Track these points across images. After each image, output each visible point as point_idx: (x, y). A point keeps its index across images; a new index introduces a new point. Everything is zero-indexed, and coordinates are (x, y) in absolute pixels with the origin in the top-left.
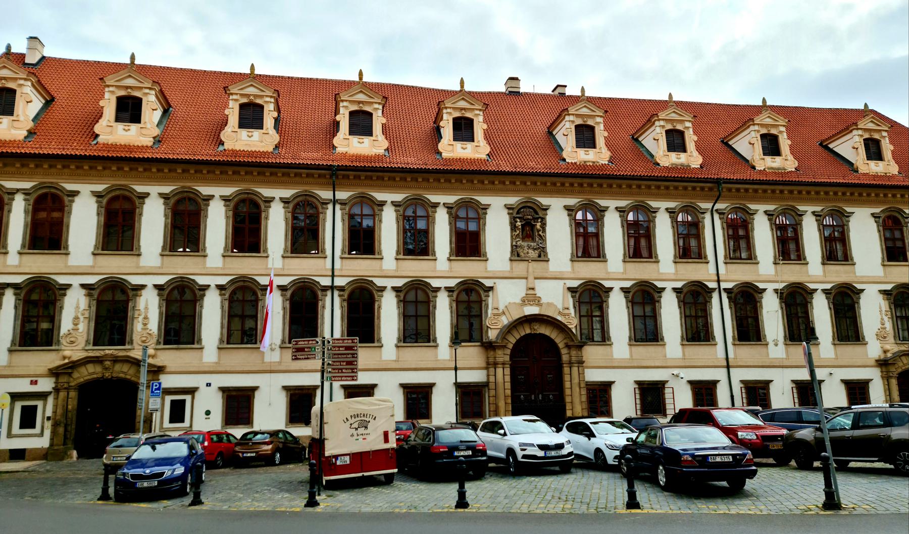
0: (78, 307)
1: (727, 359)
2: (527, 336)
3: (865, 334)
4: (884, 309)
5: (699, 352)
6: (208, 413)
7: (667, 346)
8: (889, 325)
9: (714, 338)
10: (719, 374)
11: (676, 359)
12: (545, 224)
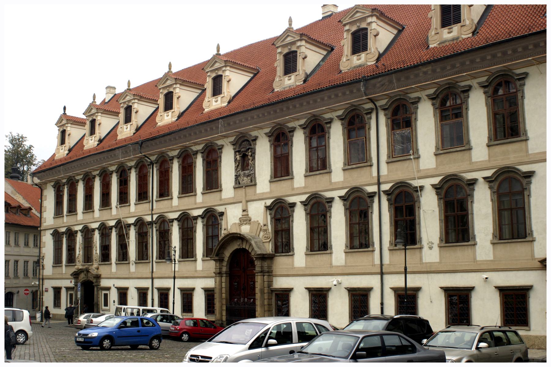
0: (80, 243)
1: (382, 265)
2: (237, 250)
6: (114, 302)
7: (334, 255)
9: (373, 245)
10: (373, 282)
11: (339, 266)
12: (254, 153)
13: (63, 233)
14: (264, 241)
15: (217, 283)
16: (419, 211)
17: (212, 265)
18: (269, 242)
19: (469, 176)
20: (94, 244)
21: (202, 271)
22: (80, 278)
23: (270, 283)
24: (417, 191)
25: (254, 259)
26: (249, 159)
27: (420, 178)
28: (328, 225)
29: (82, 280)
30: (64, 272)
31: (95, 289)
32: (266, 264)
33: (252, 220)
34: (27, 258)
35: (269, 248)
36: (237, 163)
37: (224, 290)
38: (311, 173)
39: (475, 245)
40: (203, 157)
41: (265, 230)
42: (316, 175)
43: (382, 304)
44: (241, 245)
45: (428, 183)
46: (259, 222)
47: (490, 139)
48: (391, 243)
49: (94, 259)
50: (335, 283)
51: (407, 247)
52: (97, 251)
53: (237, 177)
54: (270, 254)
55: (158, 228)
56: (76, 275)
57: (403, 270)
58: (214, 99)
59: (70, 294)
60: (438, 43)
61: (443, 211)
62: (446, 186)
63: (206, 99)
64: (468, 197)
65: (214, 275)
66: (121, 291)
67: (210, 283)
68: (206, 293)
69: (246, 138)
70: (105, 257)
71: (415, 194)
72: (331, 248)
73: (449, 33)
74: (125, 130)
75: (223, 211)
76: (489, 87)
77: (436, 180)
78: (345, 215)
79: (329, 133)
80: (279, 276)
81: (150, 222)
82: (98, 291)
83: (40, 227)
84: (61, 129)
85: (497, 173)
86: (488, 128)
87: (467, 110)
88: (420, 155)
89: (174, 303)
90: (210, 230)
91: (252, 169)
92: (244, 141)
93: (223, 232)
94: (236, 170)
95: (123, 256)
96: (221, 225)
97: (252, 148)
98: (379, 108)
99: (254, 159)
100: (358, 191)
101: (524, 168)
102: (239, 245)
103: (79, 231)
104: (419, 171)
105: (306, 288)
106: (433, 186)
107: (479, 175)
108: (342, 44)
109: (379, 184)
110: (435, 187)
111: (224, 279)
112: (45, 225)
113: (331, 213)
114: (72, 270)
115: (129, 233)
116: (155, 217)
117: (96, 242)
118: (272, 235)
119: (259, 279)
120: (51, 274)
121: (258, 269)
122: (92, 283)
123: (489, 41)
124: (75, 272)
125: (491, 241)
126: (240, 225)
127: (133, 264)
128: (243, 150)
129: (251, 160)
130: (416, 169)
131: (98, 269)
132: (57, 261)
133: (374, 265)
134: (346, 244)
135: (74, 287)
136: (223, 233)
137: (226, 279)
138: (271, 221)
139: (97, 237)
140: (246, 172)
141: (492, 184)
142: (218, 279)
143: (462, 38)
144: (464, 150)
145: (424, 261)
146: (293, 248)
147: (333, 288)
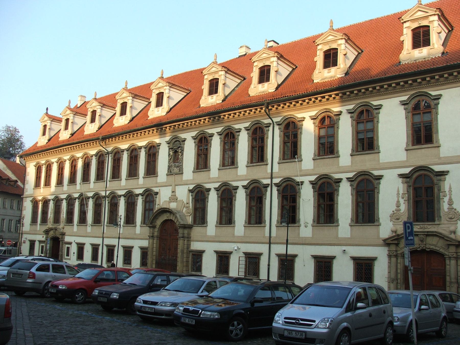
0: (51, 208)
2: (166, 221)
3: (380, 216)
4: (401, 192)
5: (255, 231)
6: (74, 253)
8: (403, 207)
10: (262, 248)
12: (183, 150)
13: (40, 201)
14: (186, 215)
15: (150, 244)
16: (299, 199)
17: (147, 230)
18: (190, 216)
19: (337, 176)
20: (62, 210)
21: (140, 234)
22: (50, 235)
23: (189, 246)
24: (299, 185)
25: (178, 228)
26: (179, 155)
27: (301, 176)
28: (233, 206)
29: (52, 236)
30: (38, 229)
31: (61, 243)
32: (186, 231)
33: (178, 199)
34: (11, 218)
35: (190, 220)
36: (170, 157)
37: (155, 249)
38: (223, 168)
39: (338, 226)
40: (145, 151)
41: (187, 207)
42: (227, 169)
43: (269, 265)
44: (169, 217)
45: (307, 179)
46: (183, 201)
47: (353, 150)
48: (278, 222)
49: (61, 221)
50: (236, 248)
51: (289, 225)
52: (64, 215)
53: (169, 167)
54: (190, 225)
55: (109, 201)
56: (47, 232)
57: (286, 242)
58: (156, 109)
59: (42, 246)
60: (320, 79)
61: (316, 201)
62: (320, 183)
63: (151, 109)
64: (335, 191)
65: (148, 238)
66: (79, 245)
67: (145, 243)
68: (142, 251)
69: (177, 139)
70: (70, 220)
71: (297, 187)
72: (234, 223)
73: (328, 73)
74: (90, 128)
75: (158, 191)
76: (354, 113)
77: (313, 178)
78: (246, 200)
79: (238, 139)
80: (196, 241)
81: (104, 196)
82: (62, 244)
83: (23, 195)
84: (44, 124)
85: (356, 175)
86: (352, 142)
87: (338, 128)
88: (302, 159)
89: (117, 257)
90: (147, 205)
91: (180, 162)
92: (176, 141)
93: (156, 207)
94: (169, 162)
95: (83, 220)
96: (156, 202)
97: (182, 147)
98: (275, 123)
99: (183, 154)
100: (256, 182)
101: (376, 173)
102: (168, 217)
103: (51, 200)
104: (301, 170)
105: (215, 251)
106: (311, 182)
107: (343, 176)
108: (251, 76)
109: (272, 178)
110: (312, 183)
111: (155, 241)
112: (26, 193)
113: (236, 197)
114: (45, 228)
115: (88, 203)
116: (108, 193)
117: (64, 208)
118: (192, 211)
119: (181, 242)
120: (29, 230)
121: (180, 235)
122: (58, 238)
123: (356, 81)
124: (47, 229)
125: (350, 224)
126: (170, 202)
127: (89, 226)
128: (175, 147)
129: (180, 155)
130: (299, 169)
131: (63, 228)
132: (34, 221)
133: (264, 237)
134: (245, 221)
135: (45, 241)
136: (157, 207)
137: (157, 242)
138: (192, 201)
139: (64, 205)
140: (176, 164)
141: (353, 183)
142: (151, 241)
143: (337, 77)
144: (334, 157)
145: (301, 236)
146: (207, 222)
147: (234, 252)
